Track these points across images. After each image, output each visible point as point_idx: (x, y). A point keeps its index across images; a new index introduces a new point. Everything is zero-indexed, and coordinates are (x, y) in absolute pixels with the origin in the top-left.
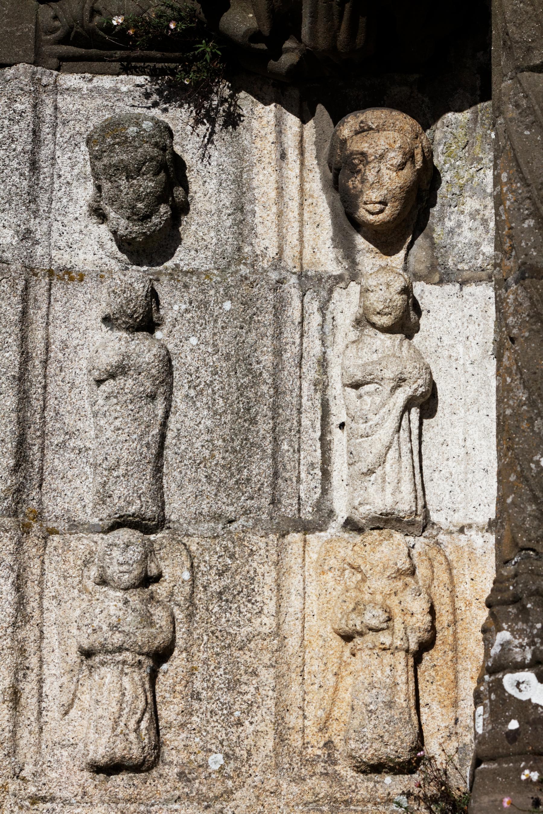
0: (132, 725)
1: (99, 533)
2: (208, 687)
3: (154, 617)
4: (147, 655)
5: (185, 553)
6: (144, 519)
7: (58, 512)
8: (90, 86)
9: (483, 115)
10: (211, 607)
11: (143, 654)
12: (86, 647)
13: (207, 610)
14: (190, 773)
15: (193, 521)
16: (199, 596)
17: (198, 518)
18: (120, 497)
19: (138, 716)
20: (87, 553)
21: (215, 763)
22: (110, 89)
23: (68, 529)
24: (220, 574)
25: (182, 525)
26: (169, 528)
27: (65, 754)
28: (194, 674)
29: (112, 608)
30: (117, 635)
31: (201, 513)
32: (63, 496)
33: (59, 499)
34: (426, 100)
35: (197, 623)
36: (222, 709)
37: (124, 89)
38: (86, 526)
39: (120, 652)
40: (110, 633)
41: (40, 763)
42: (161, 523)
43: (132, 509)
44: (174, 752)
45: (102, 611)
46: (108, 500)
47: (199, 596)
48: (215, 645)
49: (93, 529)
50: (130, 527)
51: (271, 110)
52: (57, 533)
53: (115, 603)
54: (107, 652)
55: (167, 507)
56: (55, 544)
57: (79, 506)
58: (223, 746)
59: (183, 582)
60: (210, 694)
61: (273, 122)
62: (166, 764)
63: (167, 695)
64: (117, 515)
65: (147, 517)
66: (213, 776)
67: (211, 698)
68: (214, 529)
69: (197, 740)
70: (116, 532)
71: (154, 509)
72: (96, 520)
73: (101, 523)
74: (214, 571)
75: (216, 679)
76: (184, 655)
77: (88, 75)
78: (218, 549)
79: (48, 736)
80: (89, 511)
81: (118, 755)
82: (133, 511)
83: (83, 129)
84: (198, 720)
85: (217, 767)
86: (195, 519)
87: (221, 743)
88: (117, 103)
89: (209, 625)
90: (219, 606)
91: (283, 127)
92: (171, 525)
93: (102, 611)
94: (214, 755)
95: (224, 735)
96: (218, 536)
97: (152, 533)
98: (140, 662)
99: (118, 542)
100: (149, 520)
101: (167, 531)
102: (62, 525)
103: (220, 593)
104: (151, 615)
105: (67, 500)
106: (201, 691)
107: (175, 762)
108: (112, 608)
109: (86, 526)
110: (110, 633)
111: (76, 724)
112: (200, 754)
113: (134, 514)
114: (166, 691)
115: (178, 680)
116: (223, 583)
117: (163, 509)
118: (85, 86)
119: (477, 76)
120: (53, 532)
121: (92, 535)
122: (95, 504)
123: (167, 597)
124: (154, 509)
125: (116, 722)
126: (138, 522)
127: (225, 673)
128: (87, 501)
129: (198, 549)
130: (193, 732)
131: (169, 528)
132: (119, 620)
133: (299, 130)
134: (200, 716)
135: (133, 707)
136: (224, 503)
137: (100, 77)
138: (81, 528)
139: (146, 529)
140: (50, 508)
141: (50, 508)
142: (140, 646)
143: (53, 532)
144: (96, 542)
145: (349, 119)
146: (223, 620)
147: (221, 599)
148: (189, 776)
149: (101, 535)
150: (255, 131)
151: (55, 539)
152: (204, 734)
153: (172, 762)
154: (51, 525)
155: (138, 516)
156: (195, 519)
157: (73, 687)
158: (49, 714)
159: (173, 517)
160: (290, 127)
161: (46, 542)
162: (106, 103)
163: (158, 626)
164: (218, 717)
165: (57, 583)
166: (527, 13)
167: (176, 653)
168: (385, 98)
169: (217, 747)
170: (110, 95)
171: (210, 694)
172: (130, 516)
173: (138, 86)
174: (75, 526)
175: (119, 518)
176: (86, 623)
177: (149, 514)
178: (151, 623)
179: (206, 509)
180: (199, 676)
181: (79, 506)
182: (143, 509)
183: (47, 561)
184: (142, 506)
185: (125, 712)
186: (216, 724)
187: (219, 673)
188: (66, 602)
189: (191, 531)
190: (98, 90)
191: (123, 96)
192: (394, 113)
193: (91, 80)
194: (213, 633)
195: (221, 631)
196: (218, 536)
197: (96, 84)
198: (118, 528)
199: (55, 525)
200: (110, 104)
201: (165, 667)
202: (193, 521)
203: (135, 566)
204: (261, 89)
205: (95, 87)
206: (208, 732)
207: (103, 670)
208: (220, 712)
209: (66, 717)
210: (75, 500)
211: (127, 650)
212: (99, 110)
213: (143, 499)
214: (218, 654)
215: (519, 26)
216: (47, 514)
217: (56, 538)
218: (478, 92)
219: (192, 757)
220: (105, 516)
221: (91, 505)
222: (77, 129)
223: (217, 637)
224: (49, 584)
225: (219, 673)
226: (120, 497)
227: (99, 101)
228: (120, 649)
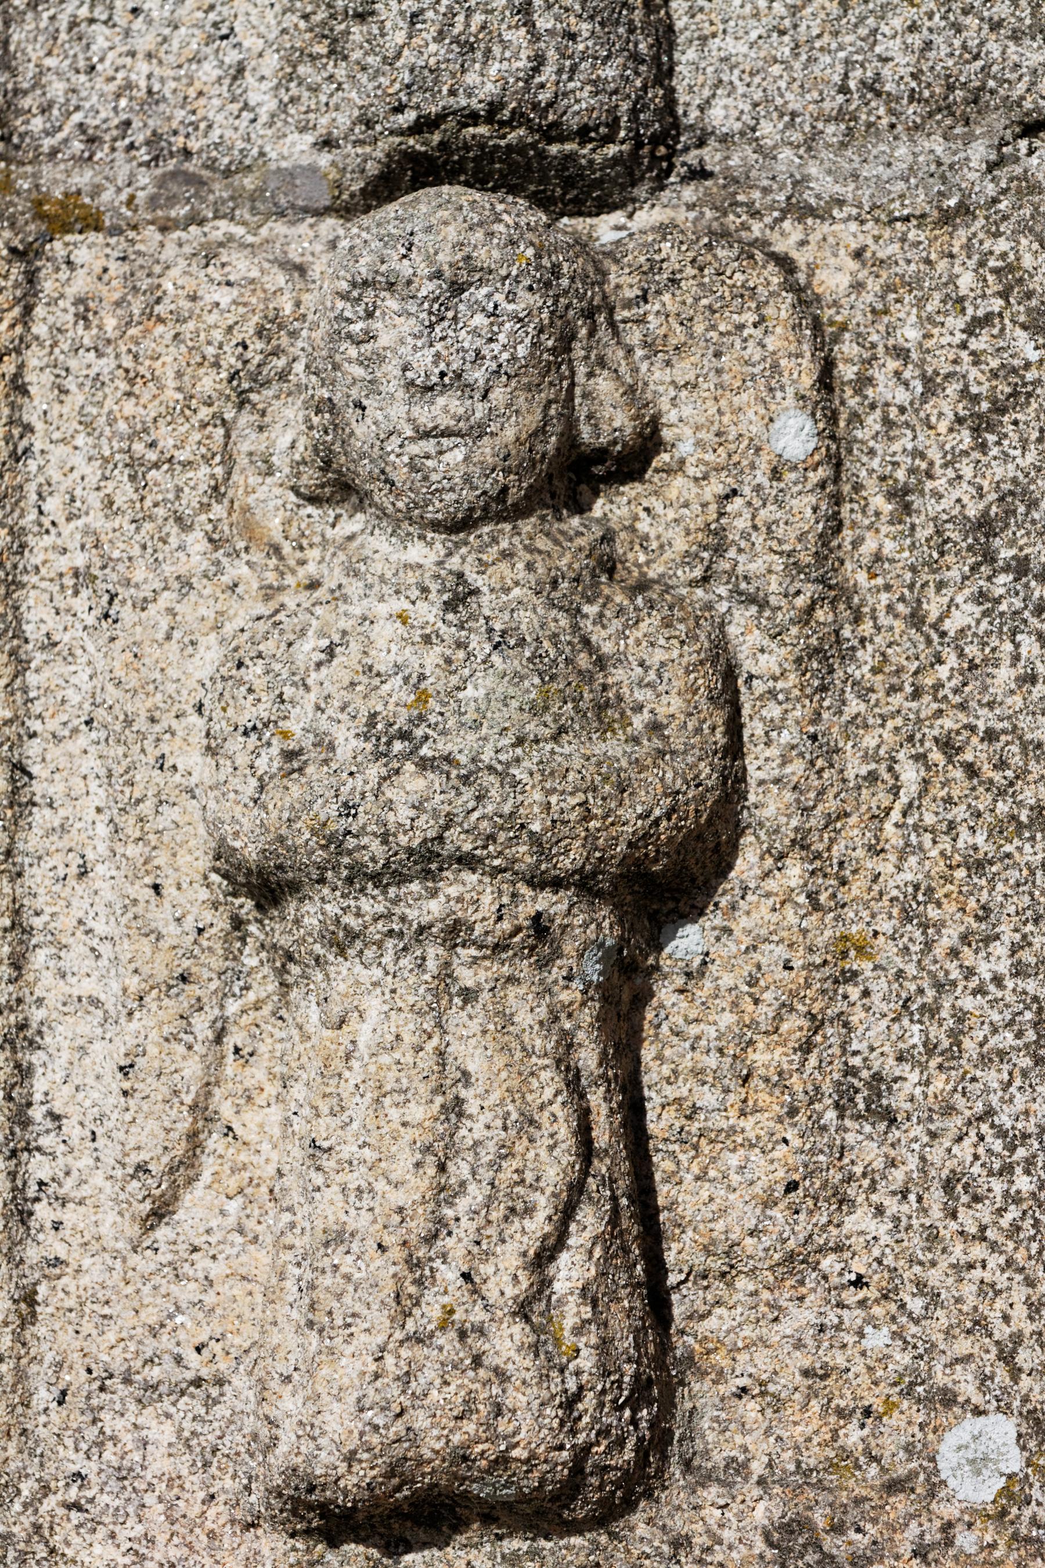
0: (505, 1276)
1: (320, 213)
2: (931, 1049)
3: (618, 674)
4: (584, 884)
5: (782, 309)
6: (554, 133)
7: (99, 108)
10: (933, 609)
11: (556, 884)
12: (251, 853)
13: (916, 619)
14: (837, 1528)
15: (832, 131)
16: (869, 546)
17: (857, 112)
18: (415, 17)
19: (539, 1224)
20: (249, 329)
21: (978, 1465)
23: (153, 202)
24: (981, 424)
25: (768, 154)
26: (699, 174)
27: (162, 1433)
28: (851, 977)
29: (385, 631)
30: (413, 783)
31: (873, 87)
32: (121, 18)
33: (101, 37)
35: (864, 692)
36: (1007, 1170)
38: (249, 182)
39: (427, 875)
40: (374, 771)
41: (27, 1488)
42: (655, 146)
43: (483, 83)
44: (750, 1409)
45: (330, 651)
46: (357, 32)
47: (869, 546)
48: (960, 812)
49: (280, 199)
50: (479, 181)
52: (92, 222)
53: (400, 604)
54: (359, 878)
55: (686, 57)
56: (81, 284)
57: (209, 71)
58: (1015, 1373)
59: (776, 474)
60: (939, 1084)
62: (707, 1479)
63: (708, 1098)
64: (409, 117)
65: (574, 123)
66: (966, 1541)
67: (949, 1110)
68: (943, 172)
69: (877, 1339)
70: (391, 209)
71: (609, 72)
72: (297, 148)
73: (324, 160)
74: (946, 405)
75: (968, 1003)
76: (795, 872)
78: (966, 281)
79: (66, 1339)
80: (261, 95)
81: (431, 1444)
82: (490, 89)
84: (882, 1229)
85: (984, 1491)
86: (839, 116)
87: (1007, 1357)
89: (927, 705)
90: (981, 597)
92: (711, 156)
93: (330, 651)
94: (971, 1425)
95: (1020, 1312)
96: (964, 210)
97: (604, 207)
98: (540, 926)
99: (405, 269)
100: (583, 134)
101: (689, 193)
102: (120, 180)
103: (985, 526)
104: (601, 662)
105: (145, 42)
106: (891, 1067)
107: (757, 1468)
108: (385, 631)
109: (249, 182)
110: (374, 771)
111: (217, 1270)
112: (895, 1420)
113: (494, 107)
114: (698, 1073)
115: (765, 1013)
116: (999, 471)
117: (664, 74)
120: (73, 217)
121: (279, 228)
122: (295, 57)
123: (689, 558)
124: (609, 72)
125: (413, 1264)
126: (520, 148)
127: (1019, 971)
128: (252, 43)
129: (858, 286)
130: (851, 1296)
131: (699, 174)
132: (422, 698)
134: (892, 1205)
135: (507, 1175)
136: (996, 26)
138: (220, 190)
139: (568, 183)
140: (57, 89)
141: (57, 89)
142: (535, 839)
143: (73, 217)
144: (301, 270)
146: (1005, 674)
147: (989, 557)
148: (829, 1543)
149: (330, 225)
151: (81, 255)
152: (916, 1305)
153: (739, 1467)
154: (57, 180)
155: (518, 118)
156: (839, 116)
157: (192, 1069)
158: (70, 1216)
159: (721, 115)
161: (31, 277)
163: (638, 722)
164: (984, 1213)
165: (95, 500)
167: (747, 863)
169: (984, 1380)
171: (939, 1084)
172: (473, 118)
174: (190, 182)
175: (416, 129)
176: (248, 715)
177: (582, 104)
178: (601, 707)
179: (903, 63)
180: (880, 986)
181: (209, 71)
182: (548, 74)
183: (38, 382)
184: (539, 61)
185: (463, 1204)
186: (978, 1251)
187: (984, 970)
188: (143, 605)
189: (823, 185)
194: (948, 745)
195: (991, 735)
196: (964, 210)
198: (415, 185)
199: (83, 178)
201: (688, 941)
202: (832, 131)
203: (498, 395)
206: (935, 1299)
207: (346, 974)
208: (998, 1186)
209: (163, 1233)
210: (188, 39)
211: (468, 861)
213: (544, 23)
214: (978, 866)
216: (37, 124)
217: (88, 251)
219: (853, 1436)
220: (343, 120)
221: (272, 62)
223: (972, 771)
224: (53, 505)
225: (984, 970)
226: (415, 17)
228: (428, 862)
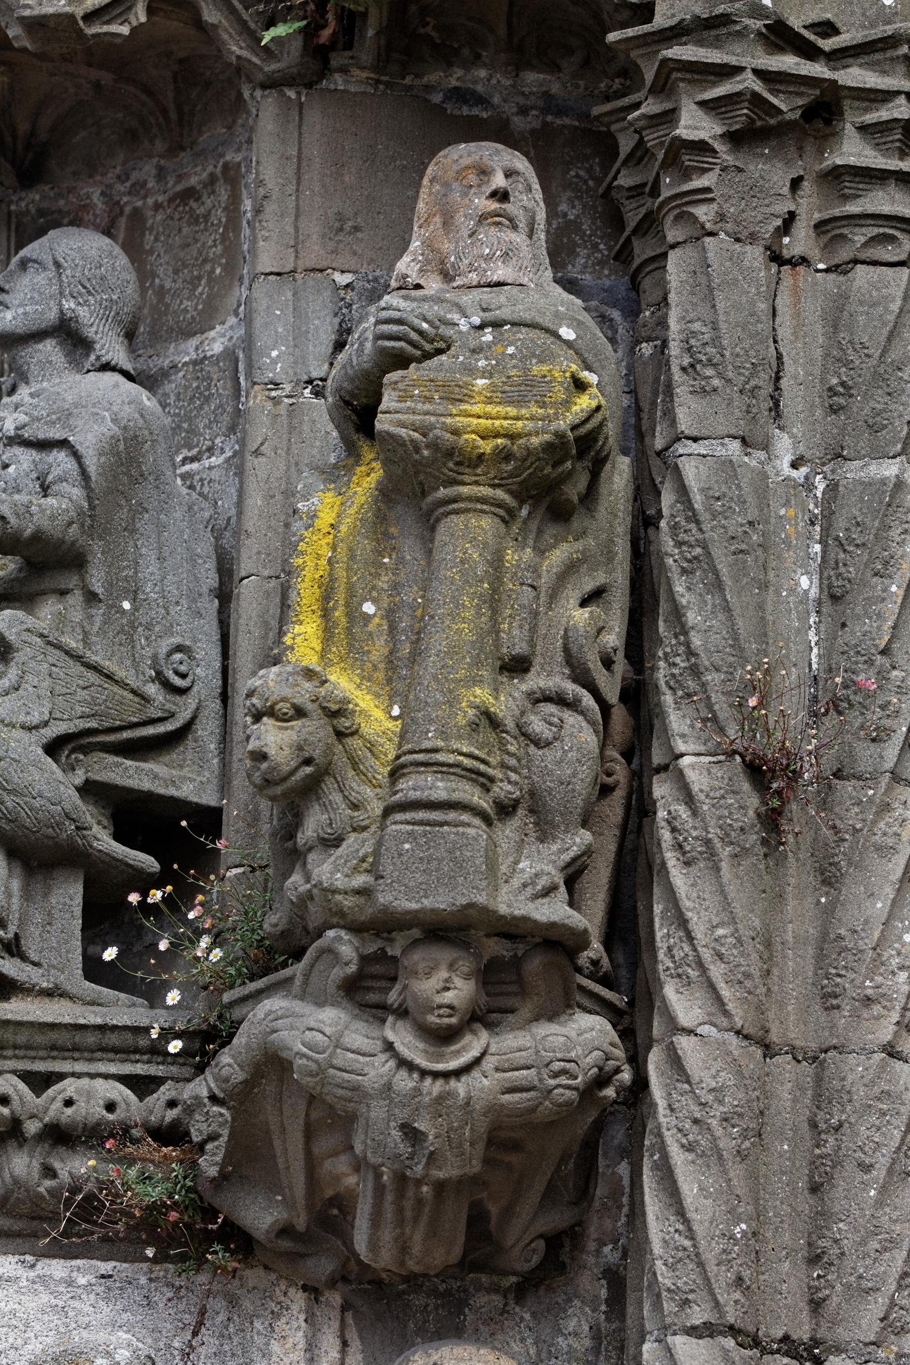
8: (32, 1274)
9: (609, 1343)
22: (62, 1281)
34: (527, 1316)
37: (82, 1281)
51: (299, 1327)
61: (302, 1345)
77: (29, 1258)
83: (20, 1342)
88: (71, 1302)
91: (316, 1352)
118: (25, 1274)
119: (604, 1282)
133: (338, 1356)
137: (47, 1261)
145: (416, 1358)
150: (274, 1358)
160: (326, 1352)
162: (54, 1302)
166: (685, 1249)
168: (466, 1310)
170: (61, 1289)
173: (103, 1277)
190: (43, 1280)
191: (80, 1291)
192: (482, 1352)
193: (33, 1266)
197: (41, 1272)
200: (61, 1304)
204: (285, 1294)
205: (39, 1276)
212: (44, 1312)
215: (672, 1267)
218: (603, 1308)
222: (11, 1340)
227: (45, 1298)
